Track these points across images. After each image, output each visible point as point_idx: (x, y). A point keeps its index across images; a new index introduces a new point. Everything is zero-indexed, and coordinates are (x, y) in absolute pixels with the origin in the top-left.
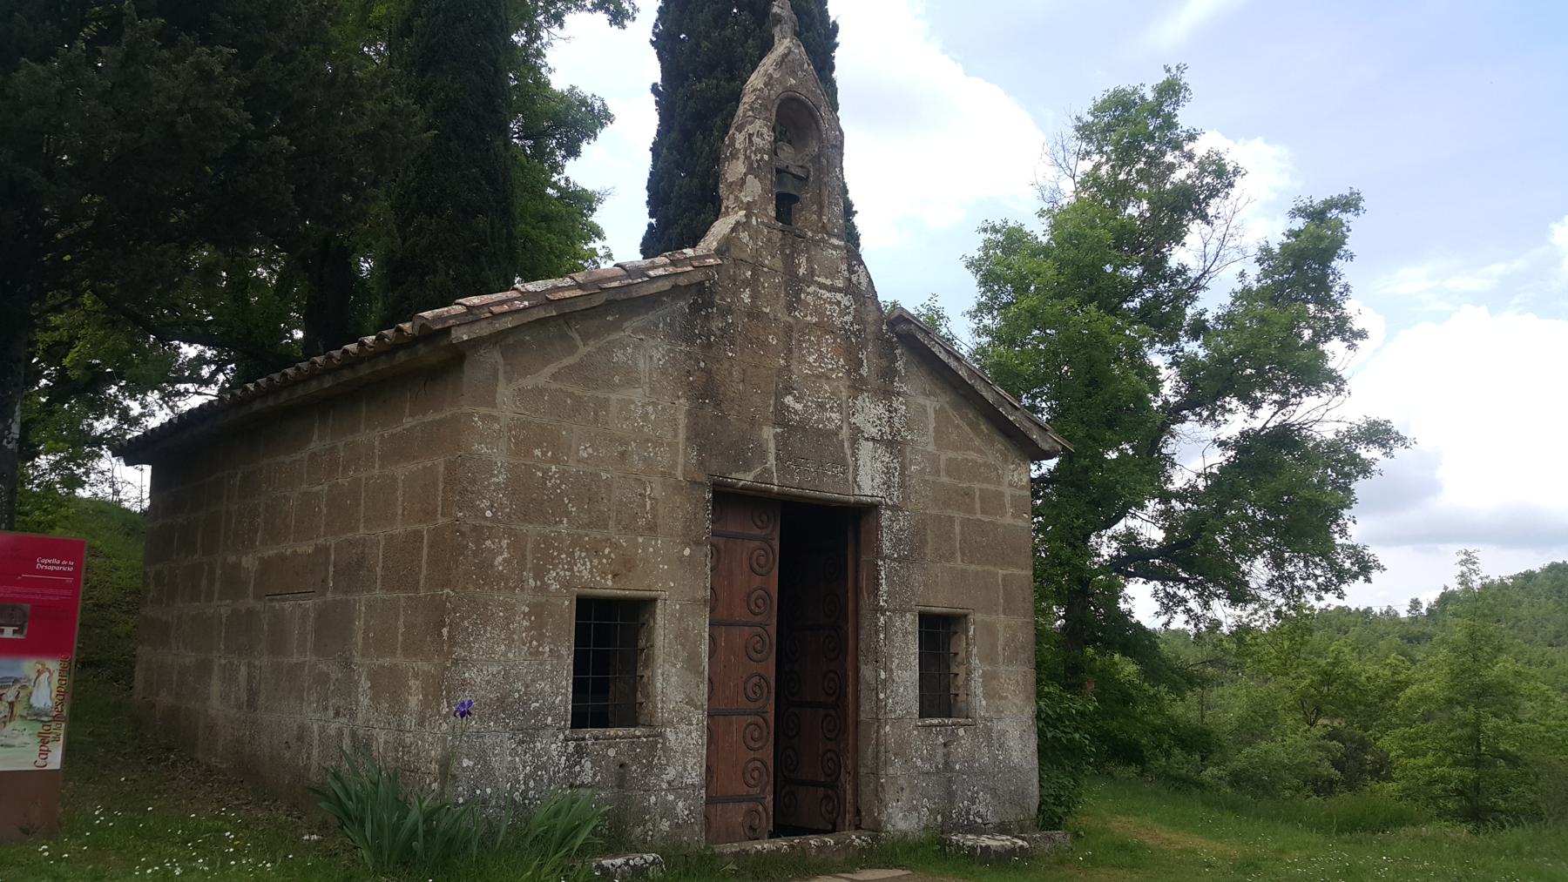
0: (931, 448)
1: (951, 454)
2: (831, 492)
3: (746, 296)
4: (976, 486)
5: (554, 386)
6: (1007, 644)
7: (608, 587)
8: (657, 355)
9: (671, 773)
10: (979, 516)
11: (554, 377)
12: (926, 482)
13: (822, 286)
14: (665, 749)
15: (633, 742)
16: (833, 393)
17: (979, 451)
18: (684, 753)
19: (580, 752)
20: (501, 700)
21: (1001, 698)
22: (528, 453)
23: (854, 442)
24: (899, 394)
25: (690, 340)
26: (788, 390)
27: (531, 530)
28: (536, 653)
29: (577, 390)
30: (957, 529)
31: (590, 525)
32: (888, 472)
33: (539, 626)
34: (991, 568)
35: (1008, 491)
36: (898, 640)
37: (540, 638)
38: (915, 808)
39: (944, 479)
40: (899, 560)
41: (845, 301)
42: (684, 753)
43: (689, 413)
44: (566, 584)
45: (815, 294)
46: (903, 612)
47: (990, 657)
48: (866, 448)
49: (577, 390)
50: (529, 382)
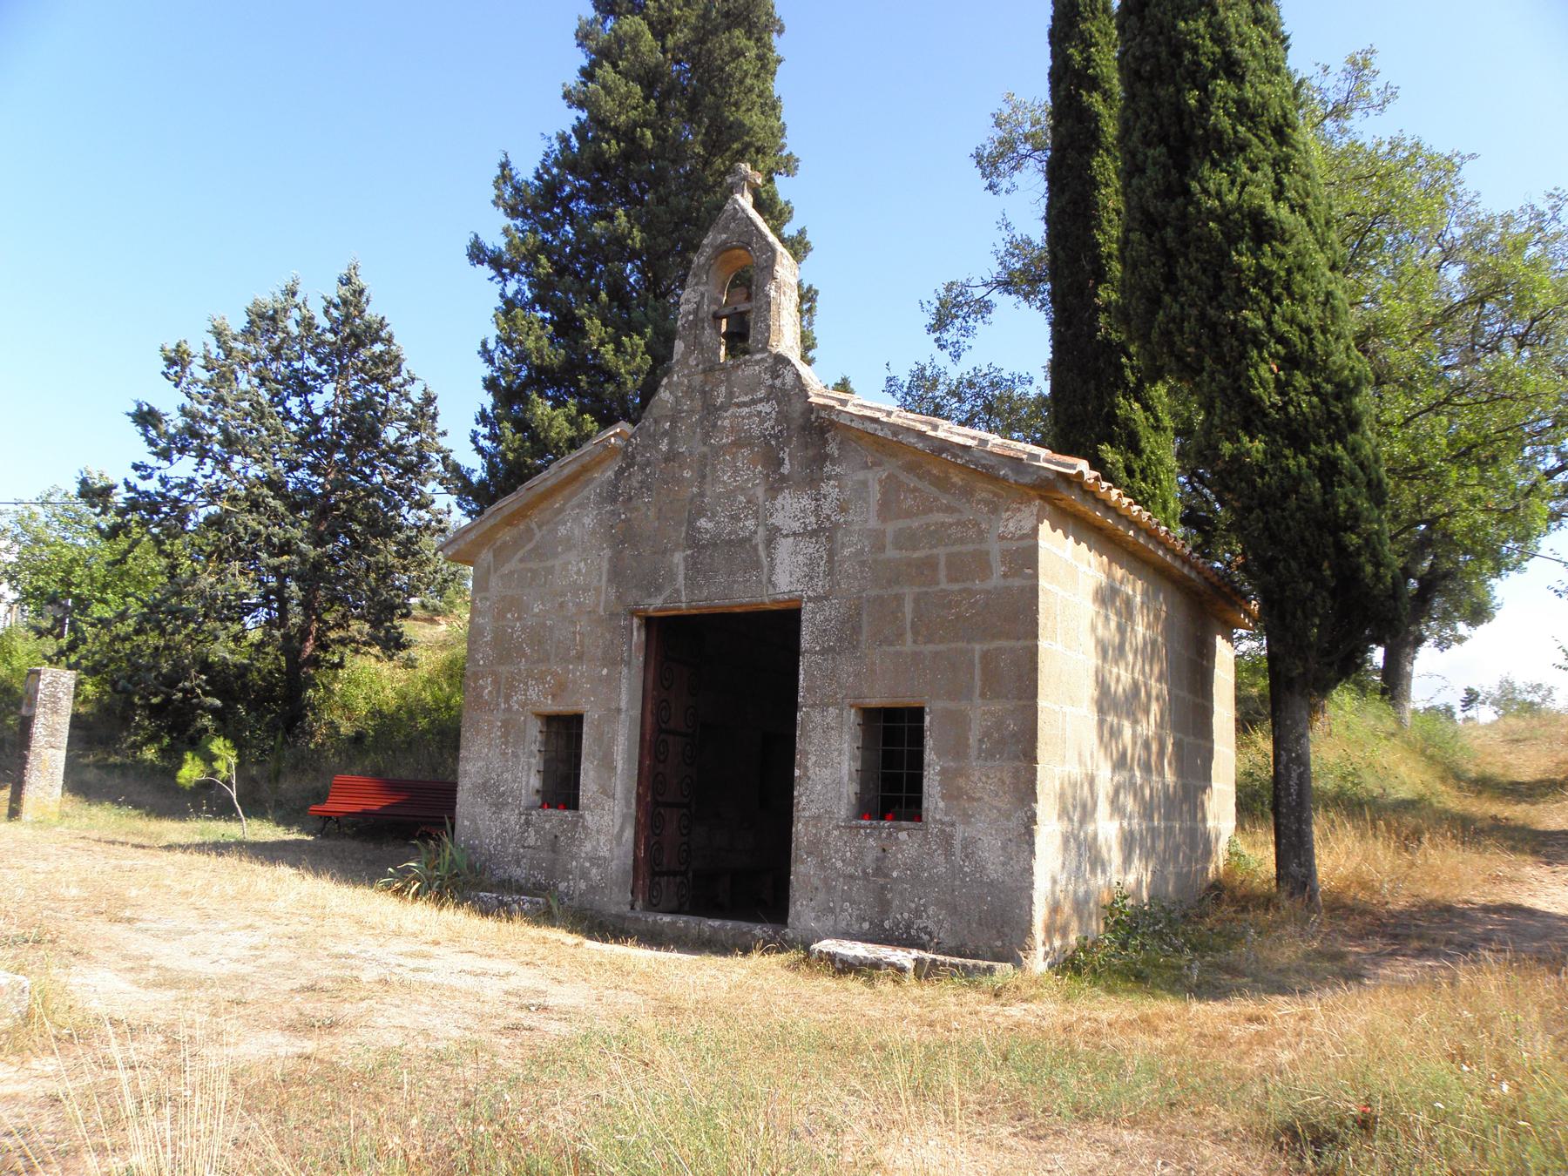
0: (874, 523)
1: (902, 523)
3: (664, 447)
4: (941, 552)
5: (522, 566)
6: (987, 734)
7: (551, 706)
8: (586, 521)
9: (588, 846)
10: (944, 585)
11: (521, 560)
12: (863, 563)
13: (739, 405)
14: (585, 828)
15: (562, 821)
16: (749, 502)
17: (949, 509)
18: (598, 832)
19: (527, 823)
20: (484, 784)
21: (971, 799)
22: (504, 617)
23: (770, 542)
24: (829, 478)
25: (614, 500)
26: (701, 513)
27: (503, 670)
28: (504, 754)
29: (533, 565)
30: (908, 608)
31: (539, 661)
32: (812, 563)
33: (506, 735)
34: (961, 645)
35: (995, 549)
36: (816, 736)
38: (832, 910)
39: (891, 553)
40: (823, 652)
41: (764, 408)
42: (598, 832)
44: (523, 705)
46: (824, 707)
47: (958, 749)
48: (785, 546)
49: (533, 565)
50: (505, 570)
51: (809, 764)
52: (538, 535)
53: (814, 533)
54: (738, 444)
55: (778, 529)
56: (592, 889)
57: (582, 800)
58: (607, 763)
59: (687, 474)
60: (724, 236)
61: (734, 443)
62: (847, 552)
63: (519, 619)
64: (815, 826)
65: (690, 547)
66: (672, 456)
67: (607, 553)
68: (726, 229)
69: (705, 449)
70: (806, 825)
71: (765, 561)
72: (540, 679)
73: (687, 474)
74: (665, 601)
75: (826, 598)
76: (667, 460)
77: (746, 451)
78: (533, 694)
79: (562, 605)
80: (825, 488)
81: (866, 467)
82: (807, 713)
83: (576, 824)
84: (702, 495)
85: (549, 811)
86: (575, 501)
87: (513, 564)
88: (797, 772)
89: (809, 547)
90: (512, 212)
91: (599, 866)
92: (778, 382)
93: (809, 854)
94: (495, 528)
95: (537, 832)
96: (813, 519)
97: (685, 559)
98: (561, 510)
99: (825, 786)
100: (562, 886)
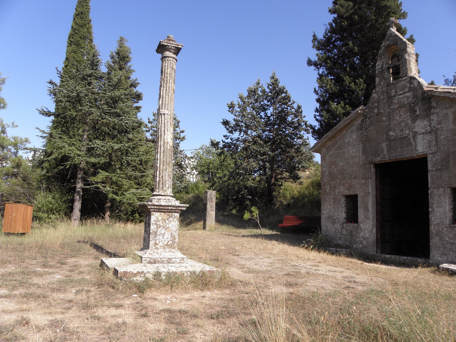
2: (406, 154)
7: (347, 193)
8: (354, 136)
9: (362, 234)
11: (335, 150)
12: (449, 140)
14: (361, 229)
15: (353, 227)
16: (406, 125)
18: (365, 230)
19: (343, 227)
20: (329, 216)
24: (433, 114)
25: (361, 129)
26: (390, 130)
28: (334, 207)
29: (339, 151)
32: (430, 142)
33: (334, 202)
37: (335, 204)
38: (446, 254)
40: (436, 170)
42: (365, 230)
43: (362, 147)
44: (339, 193)
45: (398, 98)
46: (438, 188)
48: (420, 138)
49: (339, 151)
50: (330, 153)
51: (434, 207)
52: (339, 142)
53: (429, 132)
54: (400, 107)
55: (417, 132)
56: (364, 247)
57: (359, 220)
58: (366, 209)
59: (384, 119)
60: (388, 42)
61: (399, 107)
62: (442, 137)
63: (336, 167)
64: (438, 227)
65: (387, 141)
66: (379, 114)
67: (361, 145)
68: (388, 40)
69: (389, 110)
70: (434, 226)
71: (413, 143)
72: (344, 185)
73: (384, 119)
74: (381, 159)
75: (436, 153)
76: (377, 115)
77: (403, 109)
78: (342, 189)
79: (348, 162)
80: (432, 117)
81: (447, 108)
82: (432, 190)
83: (358, 228)
84: (390, 125)
85: (349, 224)
86: (349, 131)
87: (332, 152)
88: (430, 210)
89: (428, 137)
90: (318, 49)
91: (366, 240)
92: (412, 86)
93: (436, 236)
94: (326, 142)
95: (346, 230)
96: (429, 128)
97: (386, 145)
98: (345, 134)
99: (441, 214)
100: (355, 246)
